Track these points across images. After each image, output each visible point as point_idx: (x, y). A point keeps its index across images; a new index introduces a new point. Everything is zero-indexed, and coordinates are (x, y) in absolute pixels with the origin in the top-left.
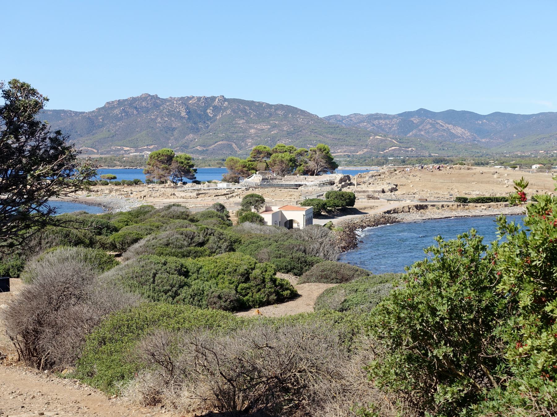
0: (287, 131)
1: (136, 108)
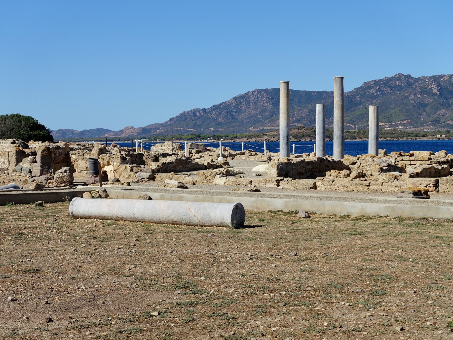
1: (390, 87)
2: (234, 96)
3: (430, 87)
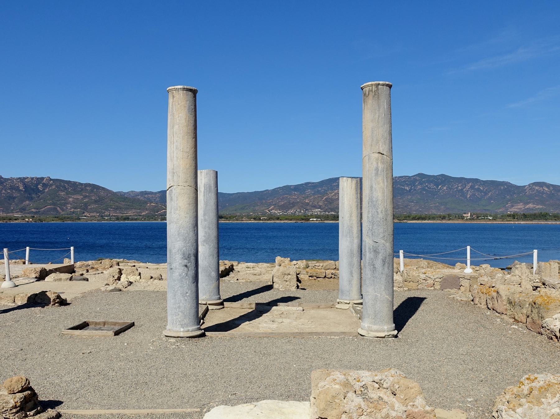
0: (95, 200)
3: (17, 185)
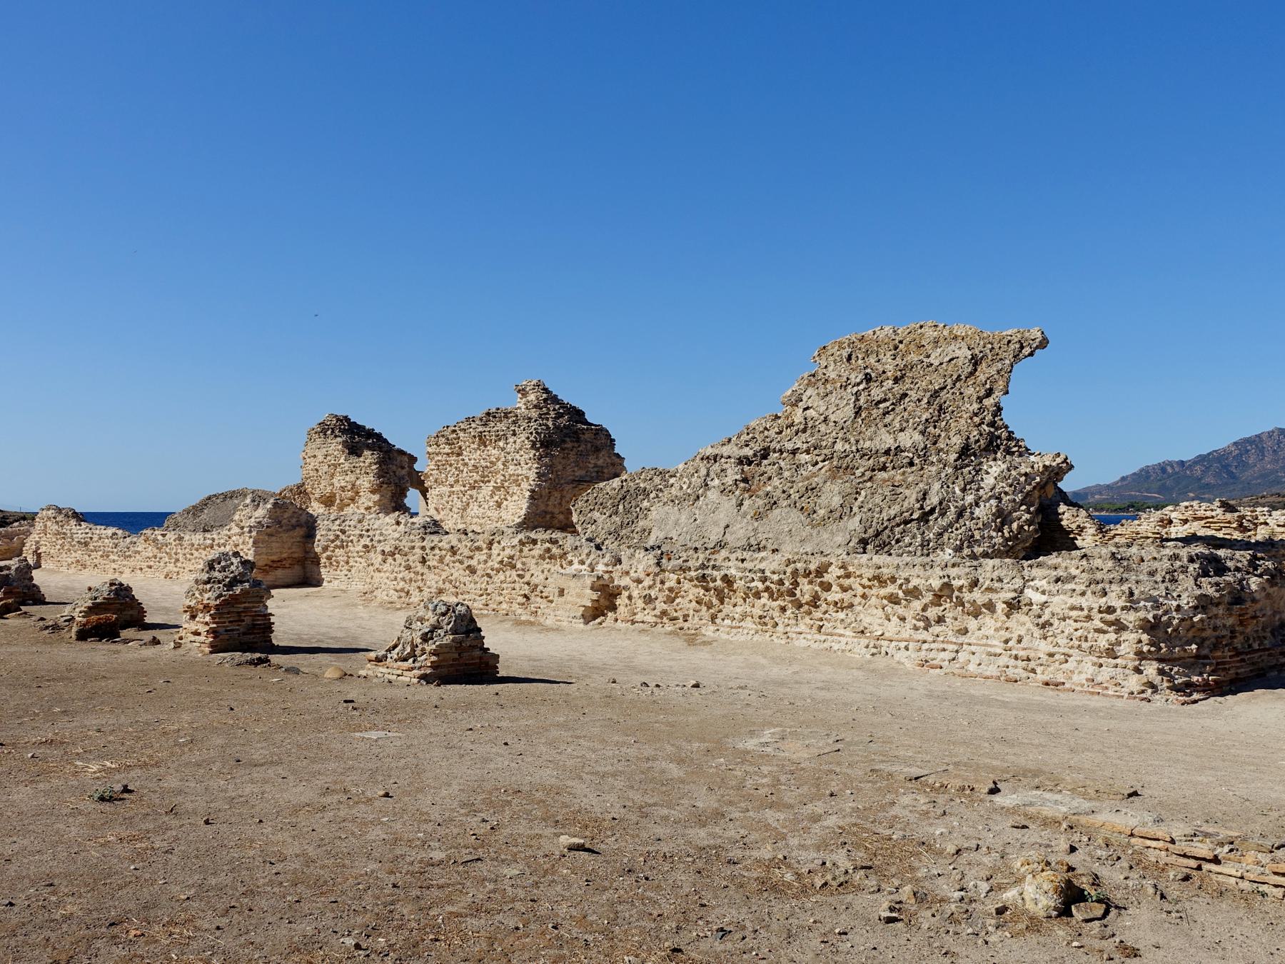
2: (1235, 441)
